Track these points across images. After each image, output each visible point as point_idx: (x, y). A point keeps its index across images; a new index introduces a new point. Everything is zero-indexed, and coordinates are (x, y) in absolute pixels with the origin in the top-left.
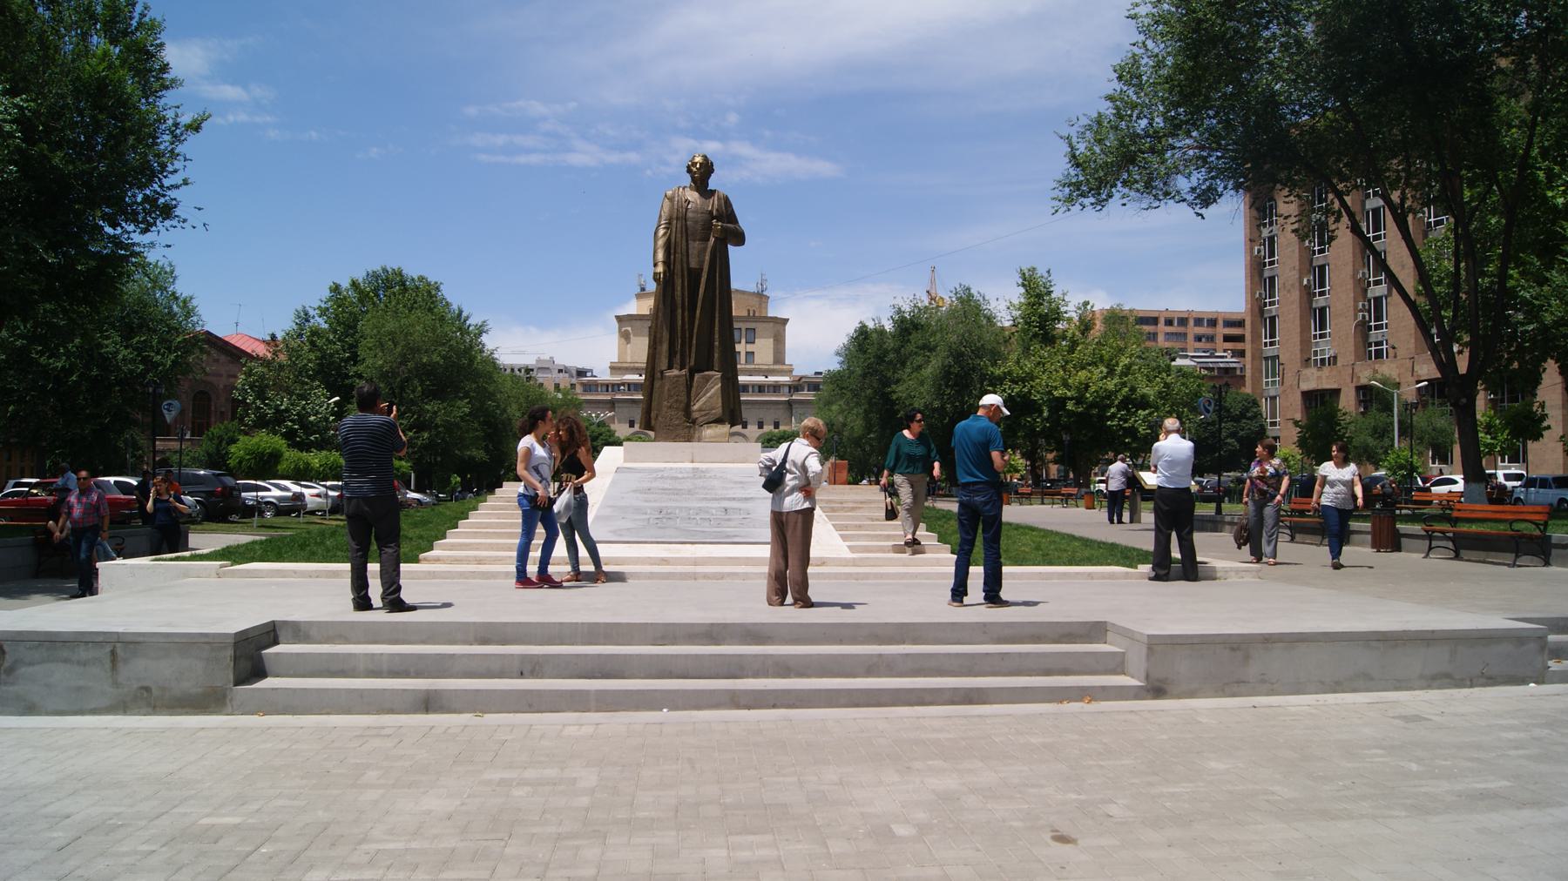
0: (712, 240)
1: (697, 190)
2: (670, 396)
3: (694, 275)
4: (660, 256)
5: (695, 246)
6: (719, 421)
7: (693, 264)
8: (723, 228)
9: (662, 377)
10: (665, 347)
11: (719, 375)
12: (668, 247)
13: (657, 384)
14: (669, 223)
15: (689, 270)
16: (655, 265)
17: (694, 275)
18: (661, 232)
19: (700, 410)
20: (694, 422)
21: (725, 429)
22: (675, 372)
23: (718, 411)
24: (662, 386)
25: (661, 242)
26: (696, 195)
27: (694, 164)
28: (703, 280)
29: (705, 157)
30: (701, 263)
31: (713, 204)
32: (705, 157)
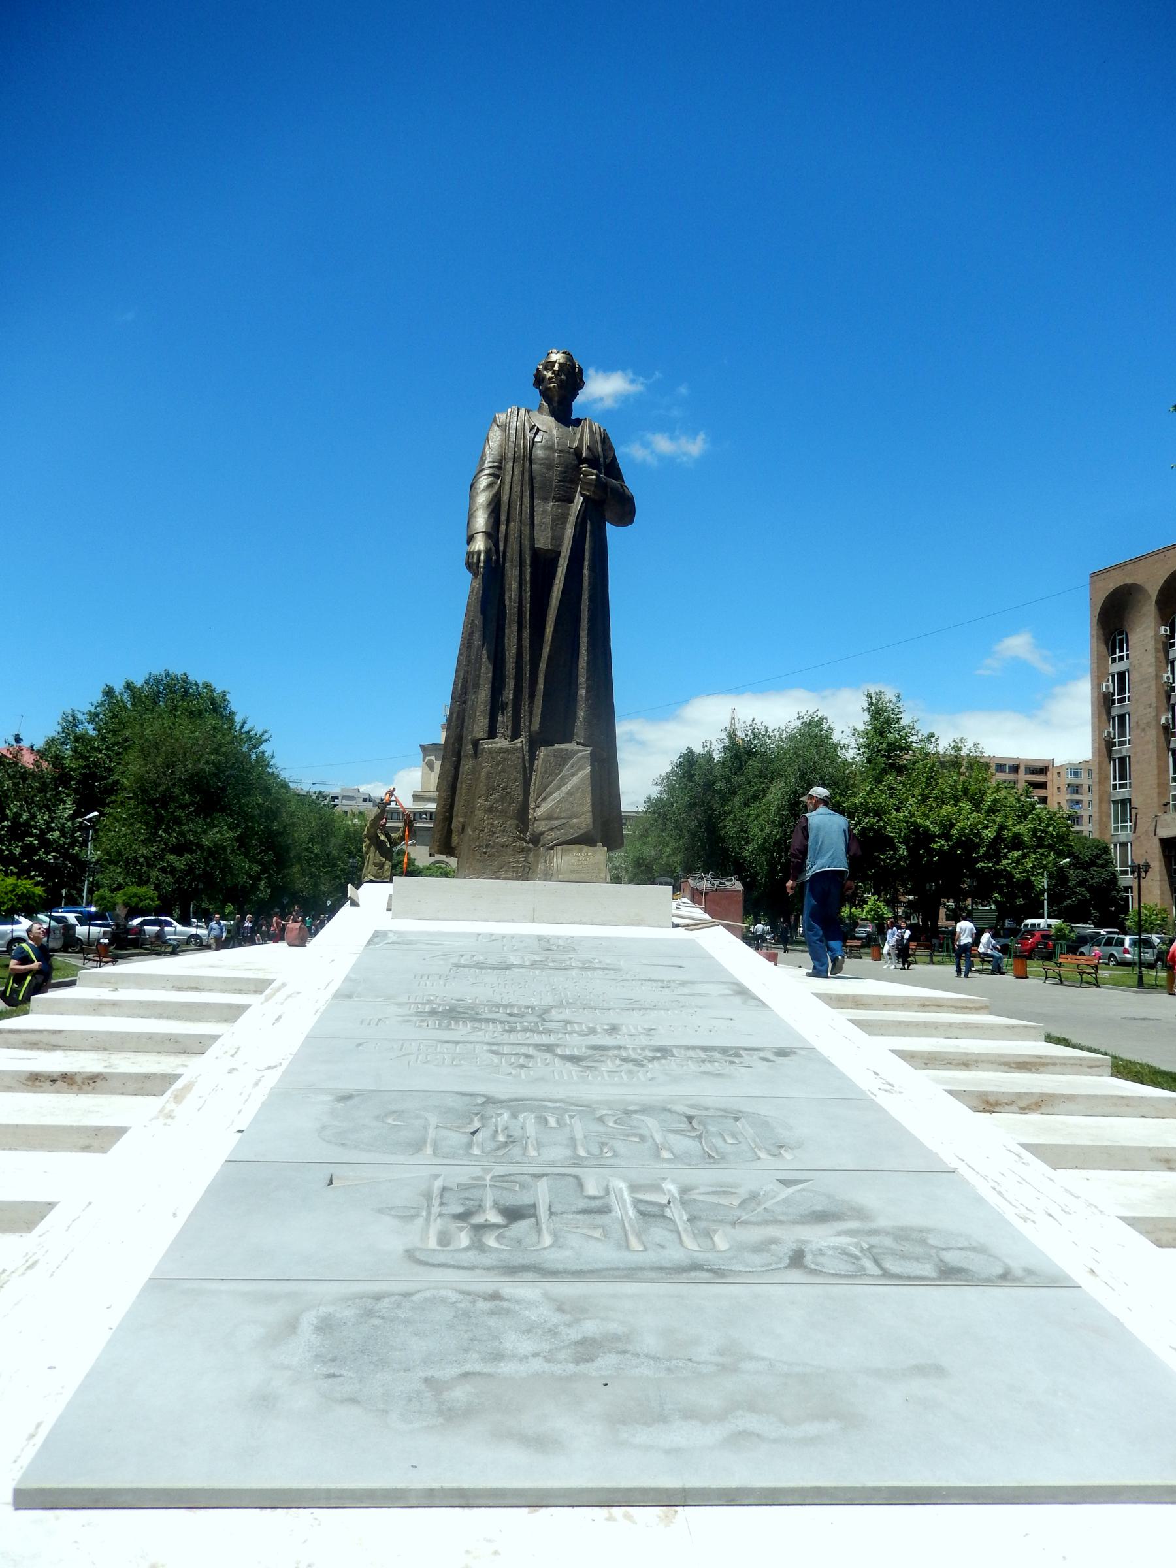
0: (579, 500)
1: (553, 413)
2: (491, 788)
3: (543, 564)
4: (481, 521)
5: (546, 510)
6: (586, 840)
7: (543, 541)
8: (599, 490)
9: (476, 752)
10: (484, 694)
11: (586, 751)
12: (495, 508)
13: (466, 766)
14: (499, 467)
15: (535, 553)
16: (471, 539)
17: (543, 564)
18: (484, 481)
19: (549, 817)
20: (536, 840)
21: (598, 855)
22: (501, 743)
23: (584, 820)
24: (475, 771)
25: (482, 499)
26: (550, 420)
27: (549, 365)
28: (561, 572)
29: (570, 357)
30: (557, 539)
31: (580, 439)
32: (570, 357)
